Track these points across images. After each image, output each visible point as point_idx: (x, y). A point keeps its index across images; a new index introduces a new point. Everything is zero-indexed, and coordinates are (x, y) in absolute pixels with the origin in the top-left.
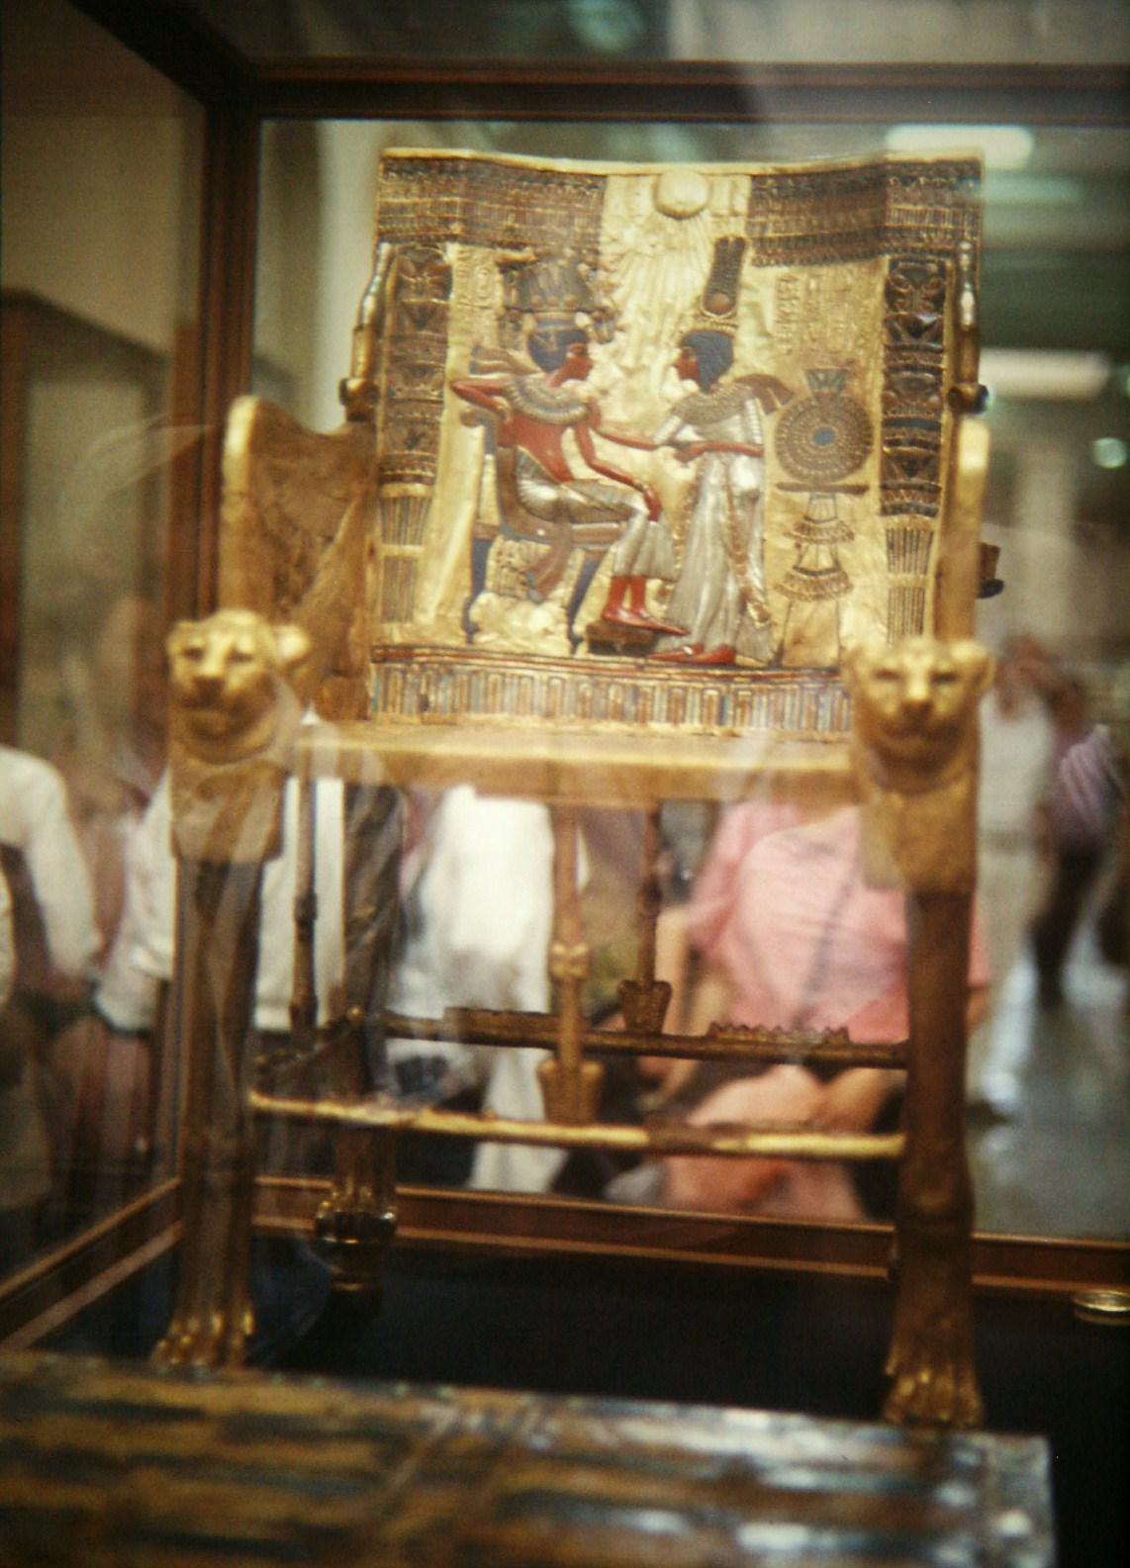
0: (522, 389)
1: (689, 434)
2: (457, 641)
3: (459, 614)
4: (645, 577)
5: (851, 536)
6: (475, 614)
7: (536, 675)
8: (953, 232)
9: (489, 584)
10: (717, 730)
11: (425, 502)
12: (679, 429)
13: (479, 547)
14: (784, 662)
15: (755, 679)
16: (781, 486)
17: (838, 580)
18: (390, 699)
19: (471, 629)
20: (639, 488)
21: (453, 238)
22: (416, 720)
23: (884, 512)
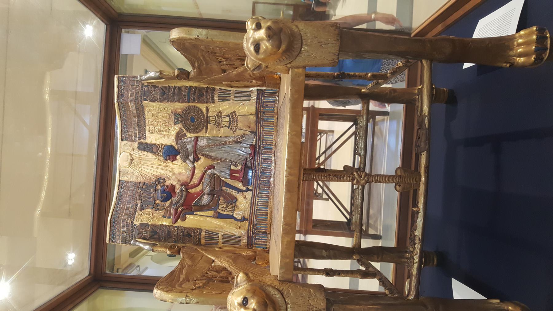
0: (177, 203)
1: (191, 158)
2: (247, 223)
4: (230, 170)
5: (220, 112)
6: (239, 217)
8: (137, 83)
9: (231, 214)
11: (207, 232)
12: (190, 161)
13: (220, 216)
14: (255, 131)
16: (206, 132)
17: (232, 116)
18: (263, 243)
19: (244, 219)
20: (206, 171)
22: (269, 235)
23: (213, 102)
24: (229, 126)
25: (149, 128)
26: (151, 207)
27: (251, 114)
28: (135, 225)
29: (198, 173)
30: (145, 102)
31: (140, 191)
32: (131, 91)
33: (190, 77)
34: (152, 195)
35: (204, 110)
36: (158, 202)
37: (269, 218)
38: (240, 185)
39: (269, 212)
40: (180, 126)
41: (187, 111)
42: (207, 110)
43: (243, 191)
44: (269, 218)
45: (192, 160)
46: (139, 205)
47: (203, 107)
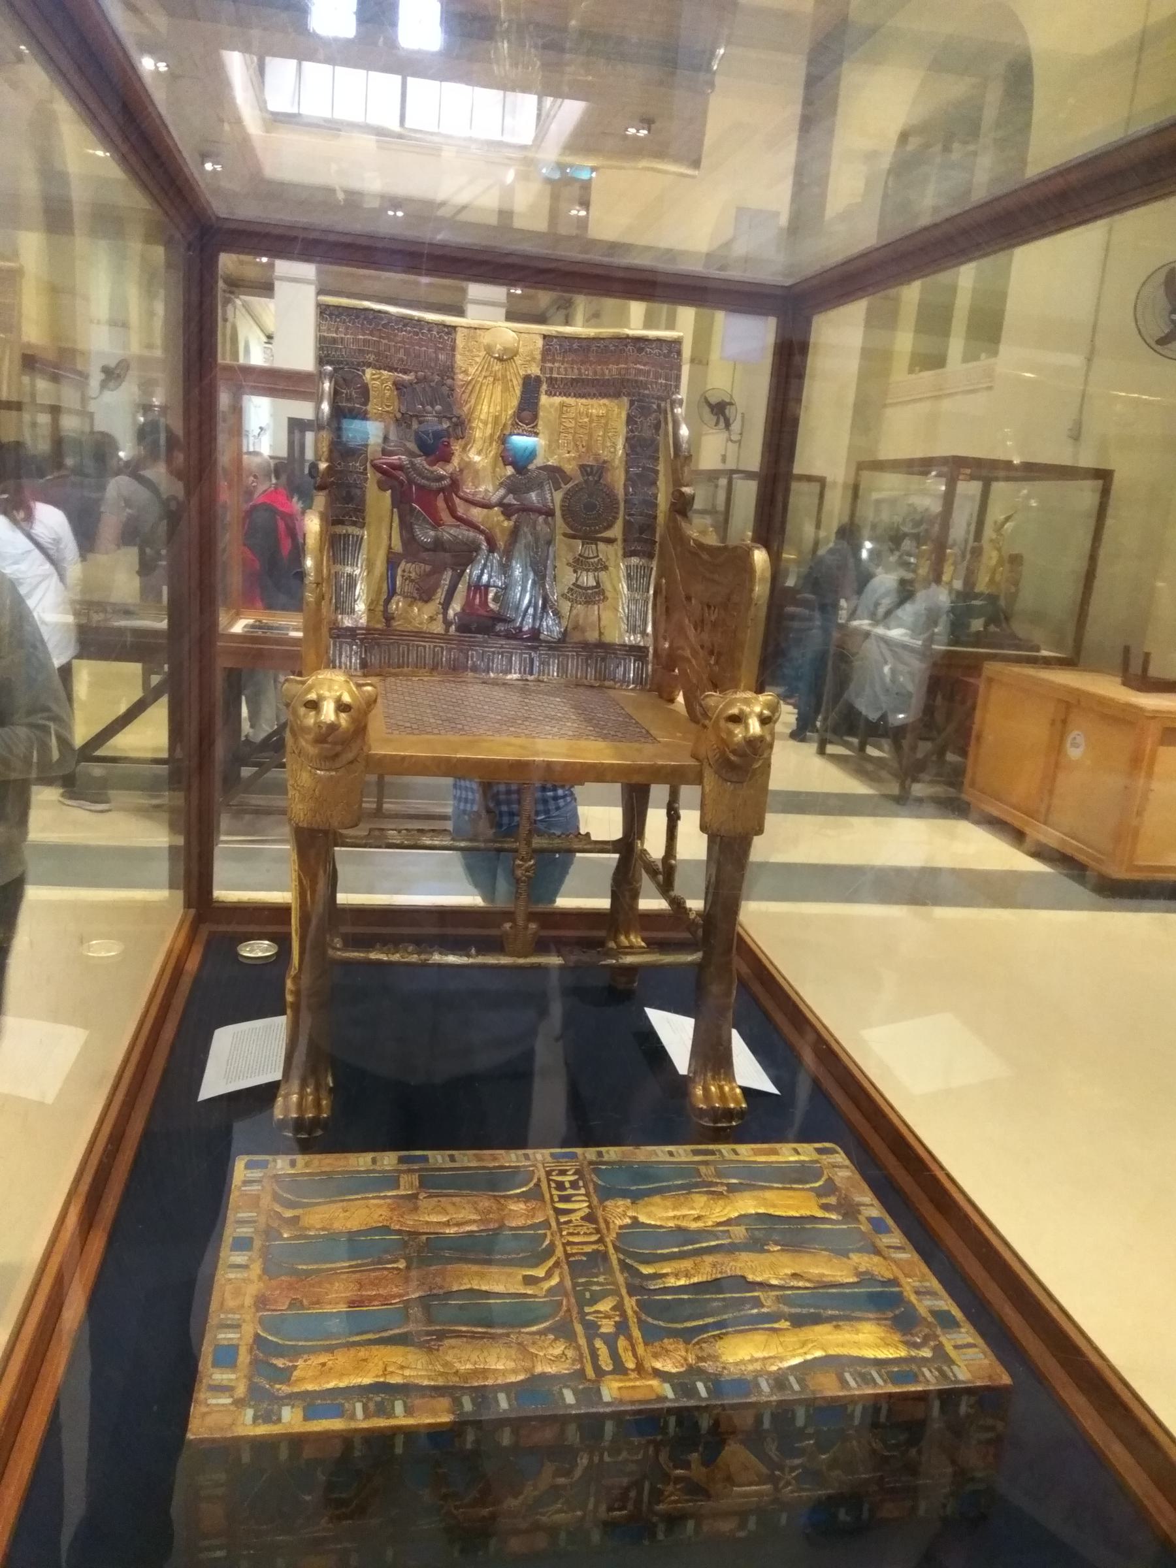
3: (381, 608)
7: (427, 644)
9: (398, 591)
10: (530, 678)
12: (504, 497)
15: (550, 648)
16: (565, 535)
17: (598, 593)
19: (389, 618)
20: (482, 532)
21: (369, 365)
22: (359, 673)
24: (579, 586)
25: (570, 406)
26: (403, 410)
27: (601, 634)
28: (364, 372)
29: (476, 514)
30: (625, 400)
31: (437, 378)
32: (649, 372)
33: (679, 518)
34: (429, 408)
35: (608, 534)
36: (415, 426)
37: (393, 671)
38: (456, 607)
39: (405, 669)
40: (579, 479)
41: (611, 496)
42: (610, 541)
43: (445, 614)
44: (393, 671)
45: (505, 501)
46: (405, 377)
47: (616, 531)
